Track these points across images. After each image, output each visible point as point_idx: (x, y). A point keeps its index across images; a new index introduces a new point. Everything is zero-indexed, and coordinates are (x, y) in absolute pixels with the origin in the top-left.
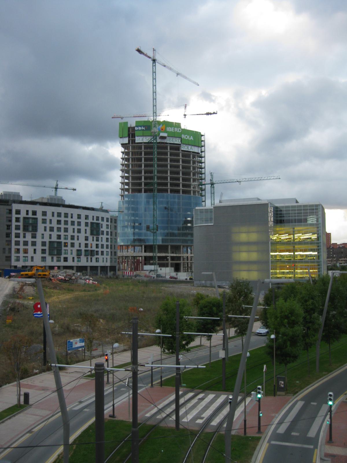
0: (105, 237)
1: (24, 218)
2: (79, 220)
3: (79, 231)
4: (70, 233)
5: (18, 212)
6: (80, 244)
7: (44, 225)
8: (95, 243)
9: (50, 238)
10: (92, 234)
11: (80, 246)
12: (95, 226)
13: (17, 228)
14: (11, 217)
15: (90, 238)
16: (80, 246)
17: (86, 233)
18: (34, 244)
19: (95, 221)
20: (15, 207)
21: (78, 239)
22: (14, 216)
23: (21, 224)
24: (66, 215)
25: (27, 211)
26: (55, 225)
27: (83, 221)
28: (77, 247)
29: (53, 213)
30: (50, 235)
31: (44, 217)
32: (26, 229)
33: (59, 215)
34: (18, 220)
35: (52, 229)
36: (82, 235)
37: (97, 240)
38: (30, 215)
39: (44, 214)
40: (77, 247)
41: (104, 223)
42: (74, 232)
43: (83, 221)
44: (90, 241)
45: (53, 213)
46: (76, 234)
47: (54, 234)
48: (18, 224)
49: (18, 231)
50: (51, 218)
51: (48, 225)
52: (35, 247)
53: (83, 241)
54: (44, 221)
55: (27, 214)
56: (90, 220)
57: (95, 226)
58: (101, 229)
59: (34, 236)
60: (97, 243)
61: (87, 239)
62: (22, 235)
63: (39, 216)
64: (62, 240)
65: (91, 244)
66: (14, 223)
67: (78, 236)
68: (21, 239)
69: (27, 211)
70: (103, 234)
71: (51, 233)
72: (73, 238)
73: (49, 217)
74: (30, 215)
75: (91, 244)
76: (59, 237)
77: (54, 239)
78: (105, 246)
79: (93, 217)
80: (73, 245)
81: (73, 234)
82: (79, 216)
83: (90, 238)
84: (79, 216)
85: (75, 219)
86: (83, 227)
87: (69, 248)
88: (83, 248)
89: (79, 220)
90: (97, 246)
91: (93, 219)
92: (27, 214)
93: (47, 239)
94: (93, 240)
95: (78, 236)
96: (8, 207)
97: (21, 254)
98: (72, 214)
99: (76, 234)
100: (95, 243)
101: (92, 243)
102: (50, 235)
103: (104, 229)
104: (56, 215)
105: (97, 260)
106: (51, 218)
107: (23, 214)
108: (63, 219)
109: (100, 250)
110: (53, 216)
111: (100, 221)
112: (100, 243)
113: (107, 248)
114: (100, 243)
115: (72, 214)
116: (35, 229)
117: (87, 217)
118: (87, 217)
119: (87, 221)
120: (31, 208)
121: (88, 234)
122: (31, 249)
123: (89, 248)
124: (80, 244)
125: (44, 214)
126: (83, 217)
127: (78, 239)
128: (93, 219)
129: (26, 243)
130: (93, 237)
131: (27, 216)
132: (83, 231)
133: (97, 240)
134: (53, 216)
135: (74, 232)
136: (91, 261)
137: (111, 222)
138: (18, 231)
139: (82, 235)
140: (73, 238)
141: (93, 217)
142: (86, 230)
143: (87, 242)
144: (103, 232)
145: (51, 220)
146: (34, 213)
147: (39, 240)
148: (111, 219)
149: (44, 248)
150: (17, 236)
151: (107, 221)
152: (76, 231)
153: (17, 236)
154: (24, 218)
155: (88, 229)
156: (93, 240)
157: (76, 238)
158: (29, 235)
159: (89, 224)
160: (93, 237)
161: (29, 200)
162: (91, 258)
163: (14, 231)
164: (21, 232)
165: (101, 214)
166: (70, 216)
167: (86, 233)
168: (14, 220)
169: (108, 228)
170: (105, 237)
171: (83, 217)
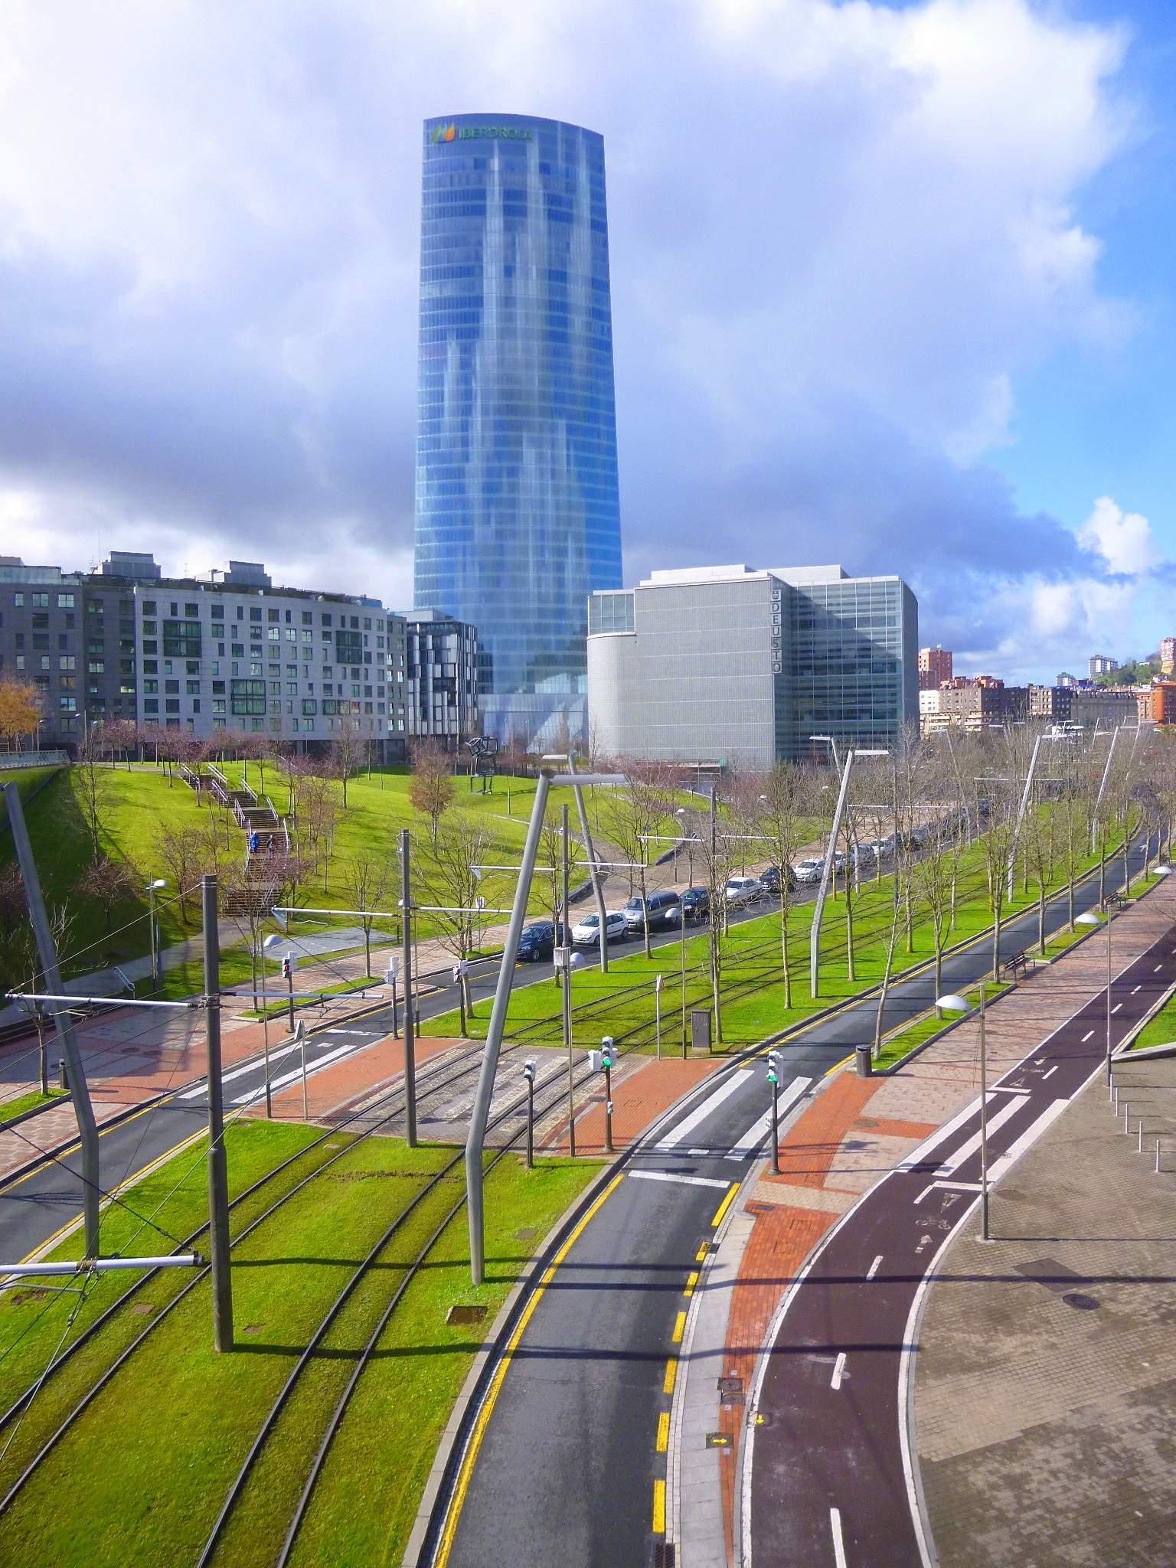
1: (166, 623)
5: (150, 607)
7: (217, 640)
12: (348, 639)
13: (150, 647)
18: (193, 685)
19: (348, 628)
22: (140, 619)
23: (158, 637)
25: (174, 606)
26: (244, 638)
29: (240, 610)
30: (236, 665)
31: (217, 621)
32: (170, 650)
33: (256, 614)
34: (149, 627)
35: (238, 649)
36: (317, 662)
37: (356, 674)
39: (218, 611)
41: (373, 635)
44: (337, 678)
45: (240, 610)
49: (151, 657)
50: (236, 622)
51: (228, 641)
52: (195, 696)
53: (318, 678)
56: (336, 626)
57: (348, 639)
58: (365, 649)
59: (192, 668)
62: (161, 666)
63: (205, 617)
65: (340, 686)
66: (140, 636)
68: (161, 676)
69: (174, 606)
70: (368, 660)
71: (235, 659)
73: (229, 617)
74: (181, 615)
75: (340, 686)
79: (343, 618)
88: (319, 694)
91: (343, 625)
93: (226, 677)
97: (163, 715)
98: (288, 613)
99: (300, 662)
103: (372, 647)
104: (246, 614)
106: (236, 622)
107: (163, 613)
110: (240, 616)
111: (361, 630)
112: (362, 682)
113: (381, 693)
115: (288, 613)
116: (196, 649)
119: (327, 629)
120: (183, 598)
121: (331, 662)
122: (185, 700)
124: (311, 686)
125: (218, 611)
128: (343, 625)
129: (172, 686)
131: (174, 618)
132: (318, 654)
133: (356, 674)
134: (240, 616)
137: (390, 630)
138: (151, 657)
141: (343, 618)
144: (369, 655)
146: (192, 609)
147: (207, 679)
148: (390, 624)
150: (151, 666)
151: (381, 628)
153: (151, 666)
154: (166, 623)
158: (180, 665)
159: (334, 636)
163: (141, 657)
164: (159, 657)
166: (282, 616)
169: (381, 645)
170: (373, 667)
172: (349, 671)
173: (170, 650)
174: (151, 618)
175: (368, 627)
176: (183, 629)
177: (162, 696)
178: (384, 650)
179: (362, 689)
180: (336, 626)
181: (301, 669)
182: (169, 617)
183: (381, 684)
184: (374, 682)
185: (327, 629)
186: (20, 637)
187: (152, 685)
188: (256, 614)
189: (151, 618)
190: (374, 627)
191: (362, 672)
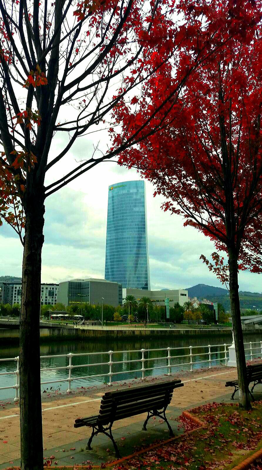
1: (18, 290)
5: (16, 288)
10: (49, 295)
13: (15, 294)
15: (48, 297)
17: (46, 295)
20: (15, 286)
22: (14, 289)
32: (18, 294)
34: (16, 291)
37: (53, 298)
61: (46, 297)
90: (52, 300)
94: (50, 298)
112: (54, 299)
117: (47, 288)
118: (47, 288)
123: (48, 301)
133: (53, 298)
150: (15, 297)
153: (15, 297)
154: (18, 290)
156: (50, 298)
167: (46, 295)
172: (51, 297)
173: (18, 294)
177: (16, 301)
182: (19, 289)
187: (15, 300)
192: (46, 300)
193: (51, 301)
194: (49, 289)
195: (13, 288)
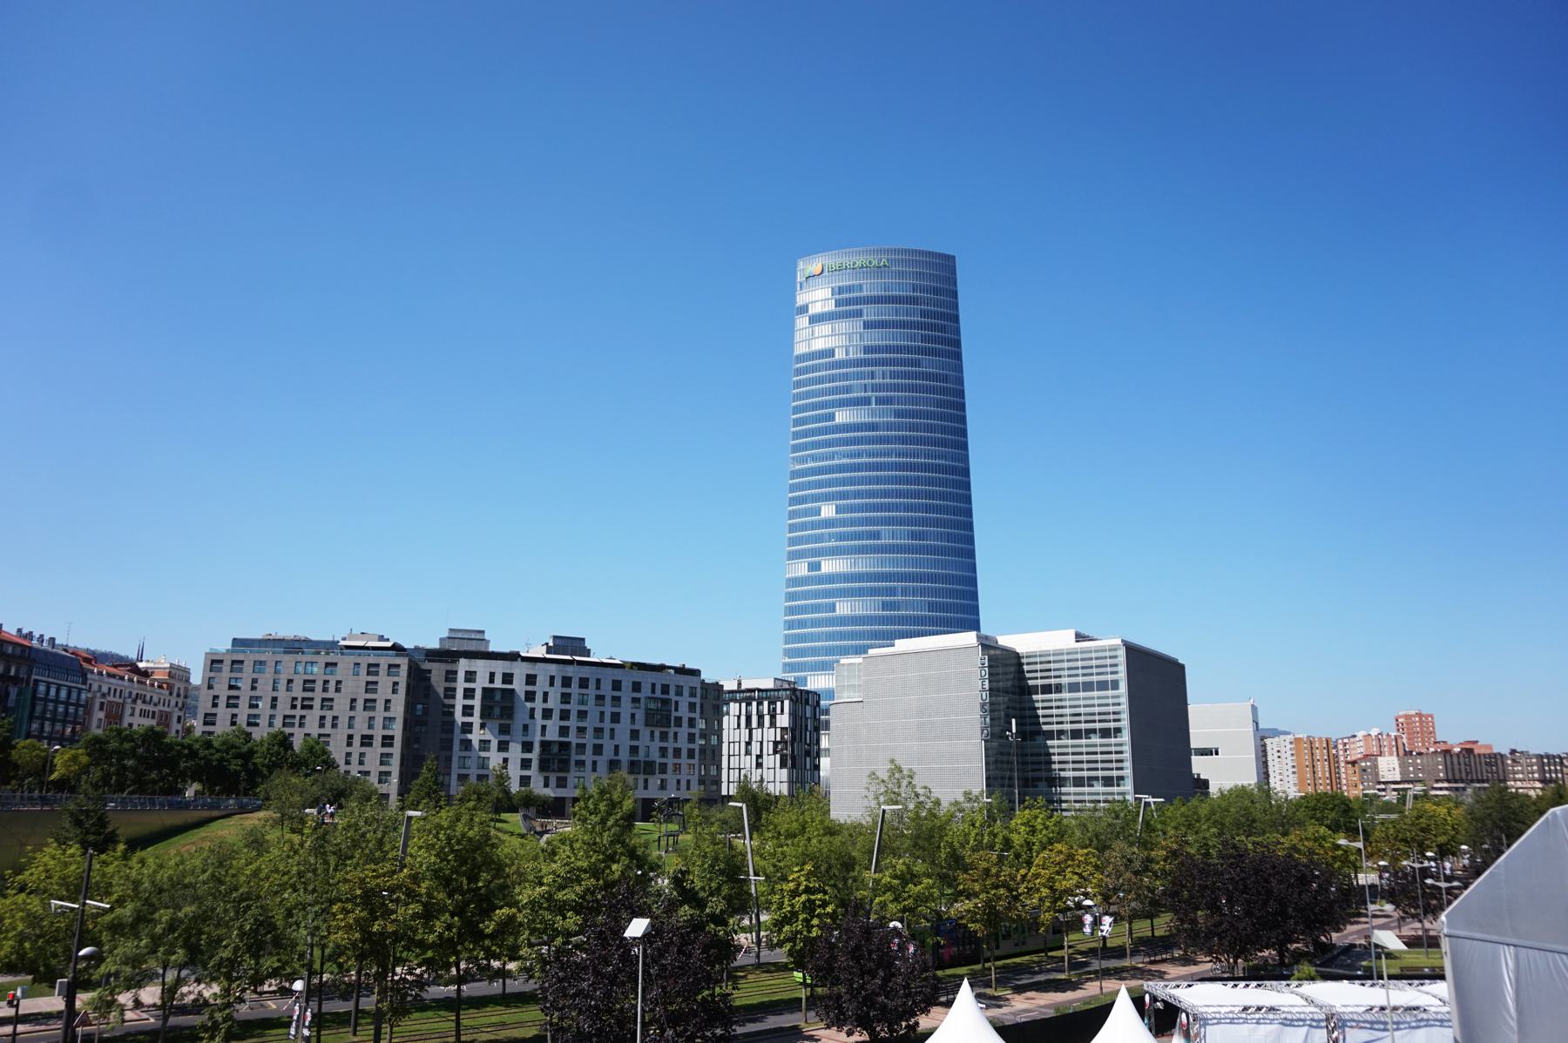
0: (684, 731)
1: (484, 689)
2: (616, 694)
3: (616, 718)
4: (591, 723)
5: (470, 676)
6: (617, 747)
8: (657, 744)
9: (543, 734)
11: (616, 753)
13: (468, 710)
14: (454, 689)
15: (645, 733)
16: (616, 753)
20: (463, 665)
21: (612, 737)
22: (461, 685)
23: (477, 702)
24: (584, 683)
25: (492, 675)
26: (554, 703)
27: (626, 694)
28: (608, 752)
31: (530, 688)
32: (486, 713)
34: (469, 693)
36: (624, 726)
37: (664, 736)
38: (498, 684)
40: (608, 752)
41: (684, 702)
42: (602, 720)
43: (626, 694)
45: (552, 678)
46: (607, 725)
47: (553, 726)
48: (469, 702)
52: (505, 755)
53: (624, 740)
54: (530, 696)
55: (492, 681)
58: (674, 714)
60: (664, 745)
61: (635, 734)
63: (519, 686)
64: (573, 738)
67: (612, 730)
69: (492, 675)
72: (598, 731)
73: (541, 686)
76: (564, 731)
77: (553, 735)
78: (684, 753)
79: (653, 685)
80: (598, 749)
81: (599, 725)
82: (617, 685)
83: (645, 733)
84: (617, 685)
85: (606, 689)
86: (626, 708)
87: (588, 757)
88: (624, 756)
89: (616, 694)
90: (663, 752)
91: (653, 691)
92: (492, 681)
95: (612, 730)
96: (450, 667)
98: (598, 681)
100: (657, 744)
101: (650, 746)
102: (544, 728)
103: (684, 712)
104: (558, 682)
105: (663, 787)
106: (547, 689)
107: (481, 683)
108: (574, 690)
109: (670, 760)
110: (552, 684)
111: (672, 696)
112: (670, 745)
114: (670, 745)
115: (598, 681)
117: (637, 687)
118: (637, 687)
119: (637, 695)
120: (500, 667)
121: (639, 725)
123: (641, 756)
124: (617, 747)
125: (531, 679)
126: (627, 685)
127: (612, 737)
128: (653, 691)
130: (652, 733)
133: (664, 736)
134: (552, 684)
135: (602, 720)
136: (646, 787)
139: (624, 726)
140: (598, 731)
141: (653, 685)
142: (633, 716)
143: (634, 743)
144: (679, 721)
145: (546, 694)
146: (508, 678)
149: (527, 756)
151: (693, 695)
152: (608, 717)
154: (484, 689)
155: (640, 716)
157: (607, 734)
160: (652, 733)
161: (506, 650)
162: (646, 781)
165: (673, 680)
166: (592, 684)
168: (460, 693)
170: (684, 731)
171: (627, 685)
172: (657, 734)
174: (471, 685)
175: (679, 693)
176: (498, 697)
178: (697, 715)
179: (671, 751)
180: (646, 691)
181: (607, 734)
182: (487, 685)
183: (692, 746)
184: (683, 743)
185: (637, 695)
186: (353, 700)
188: (567, 682)
189: (471, 685)
190: (686, 692)
191: (671, 735)
192: (634, 750)
193: (655, 756)
194: (646, 691)
195: (451, 676)
